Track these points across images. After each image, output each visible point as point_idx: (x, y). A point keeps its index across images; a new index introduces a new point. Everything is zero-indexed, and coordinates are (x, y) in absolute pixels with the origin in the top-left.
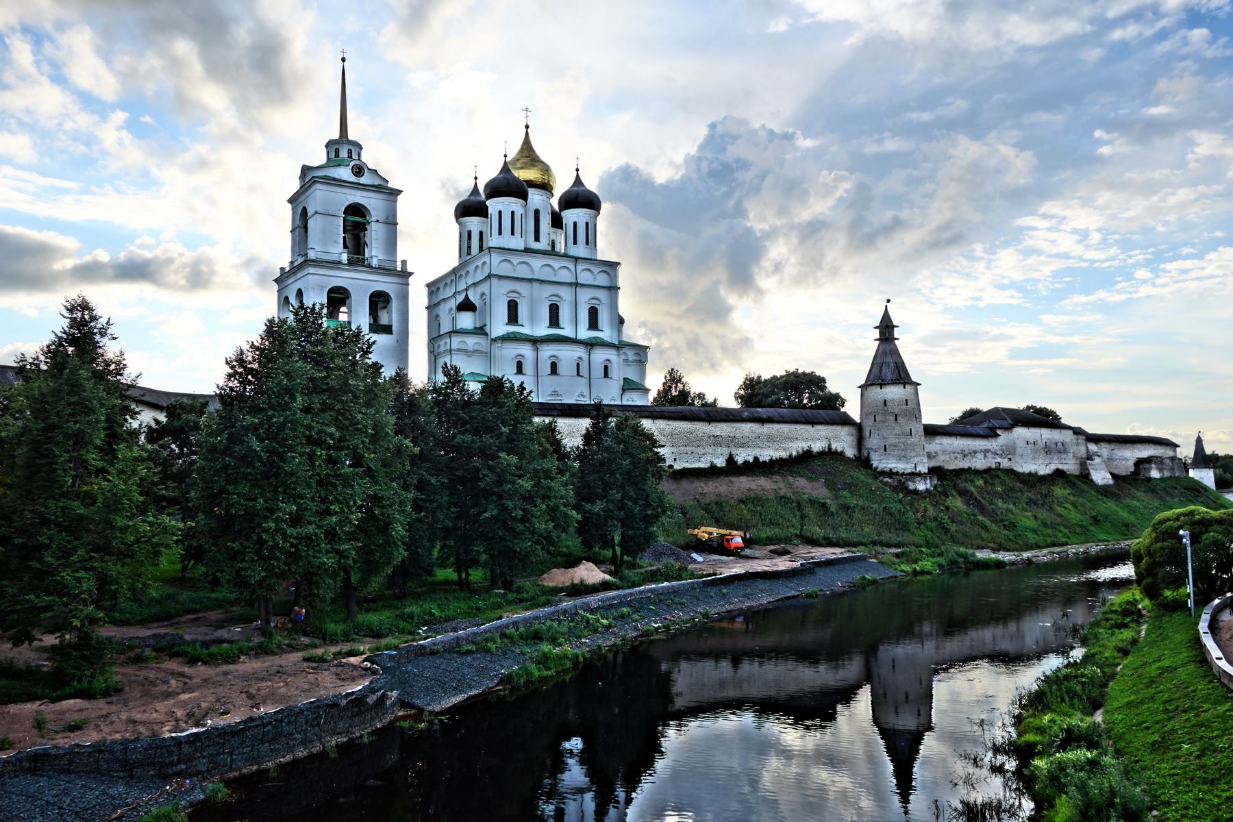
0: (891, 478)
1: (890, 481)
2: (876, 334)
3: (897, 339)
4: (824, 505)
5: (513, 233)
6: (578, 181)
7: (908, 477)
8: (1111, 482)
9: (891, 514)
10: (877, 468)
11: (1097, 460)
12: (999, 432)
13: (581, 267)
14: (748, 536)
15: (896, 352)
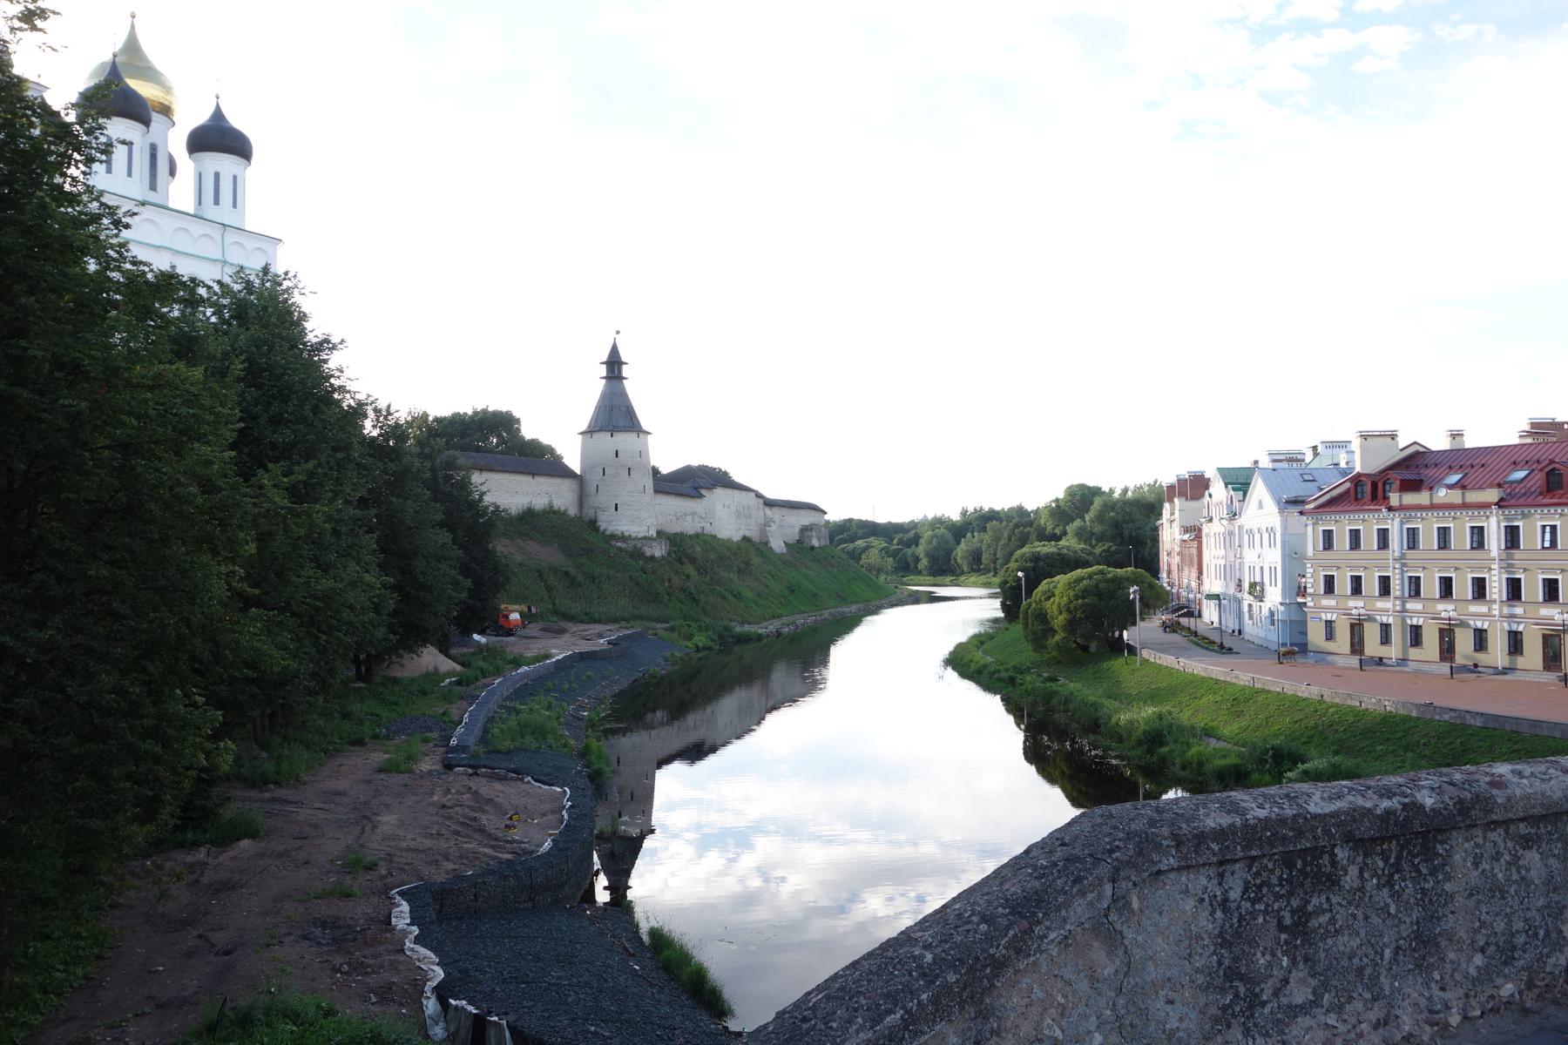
0: (624, 542)
1: (624, 546)
2: (603, 371)
3: (625, 378)
4: (567, 573)
5: (130, 174)
6: (218, 115)
7: (644, 541)
8: (785, 551)
9: (638, 584)
10: (605, 531)
11: (774, 527)
12: (703, 492)
13: (231, 237)
14: (534, 610)
15: (624, 395)
